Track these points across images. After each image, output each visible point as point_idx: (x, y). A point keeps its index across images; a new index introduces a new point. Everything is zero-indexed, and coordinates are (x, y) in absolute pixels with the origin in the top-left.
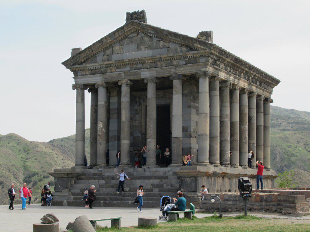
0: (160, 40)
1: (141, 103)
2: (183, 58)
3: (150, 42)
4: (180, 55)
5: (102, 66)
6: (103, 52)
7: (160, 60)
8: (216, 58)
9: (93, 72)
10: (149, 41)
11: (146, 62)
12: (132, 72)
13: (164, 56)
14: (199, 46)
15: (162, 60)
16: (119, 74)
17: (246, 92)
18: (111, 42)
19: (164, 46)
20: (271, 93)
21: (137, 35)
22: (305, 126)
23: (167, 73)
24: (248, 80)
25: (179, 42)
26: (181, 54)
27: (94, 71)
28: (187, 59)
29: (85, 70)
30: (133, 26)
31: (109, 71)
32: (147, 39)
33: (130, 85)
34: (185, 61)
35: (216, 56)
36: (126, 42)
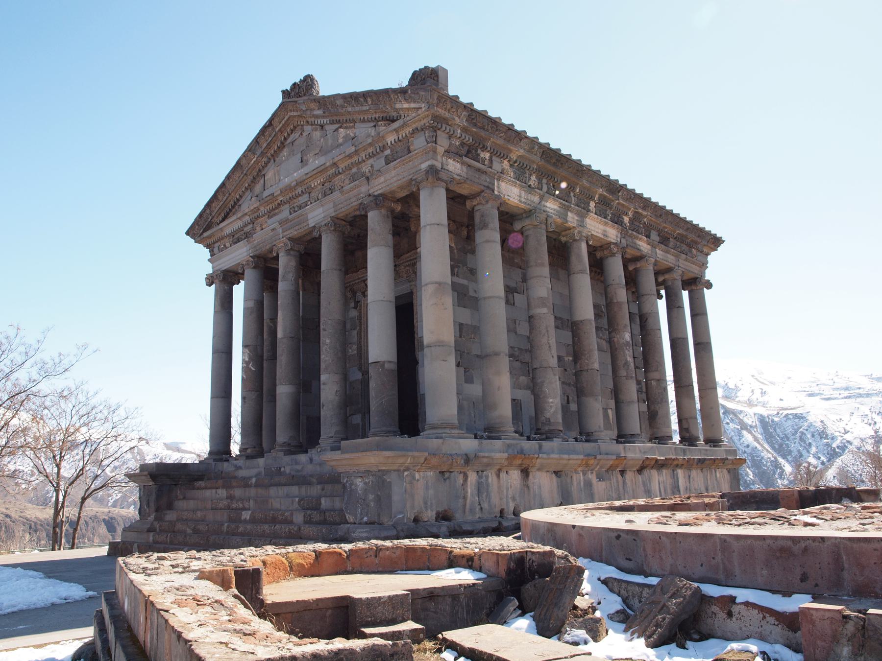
4: (370, 144)
8: (469, 139)
9: (236, 238)
10: (321, 137)
13: (340, 157)
14: (406, 105)
17: (615, 250)
18: (257, 162)
19: (346, 138)
20: (704, 265)
22: (858, 391)
24: (617, 220)
26: (370, 140)
27: (236, 236)
28: (388, 152)
29: (222, 238)
31: (258, 229)
32: (317, 134)
33: (298, 251)
35: (465, 130)
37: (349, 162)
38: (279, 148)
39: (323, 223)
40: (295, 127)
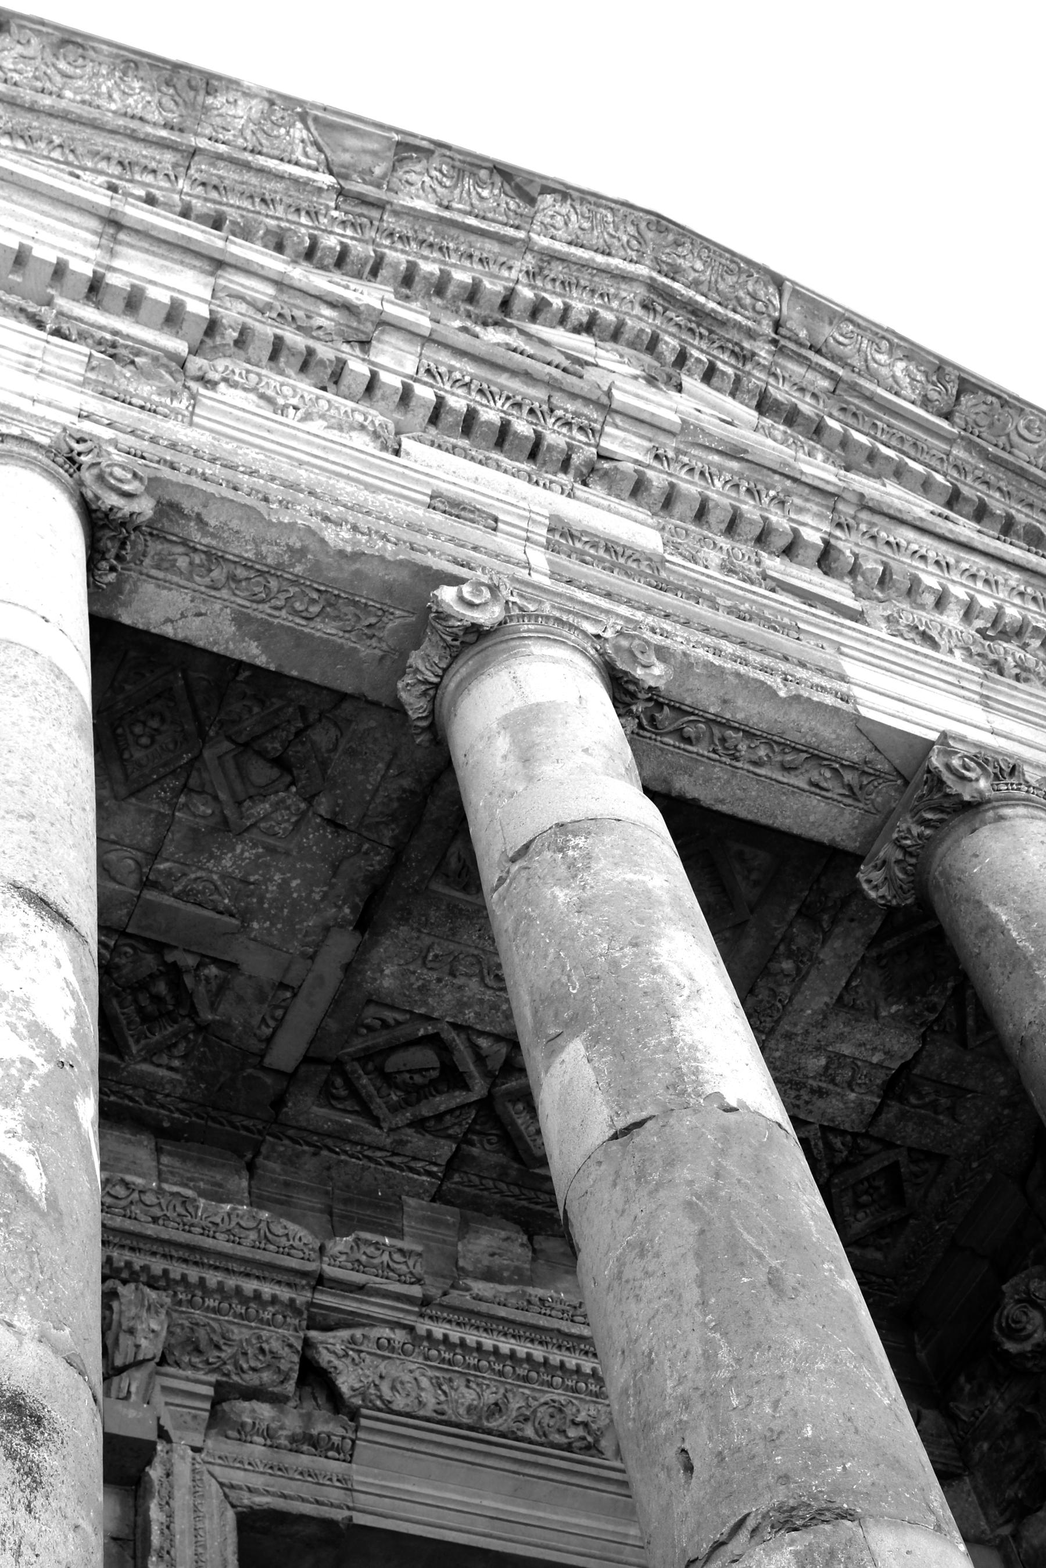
5: (132, 267)
16: (456, 508)
38: (473, 294)
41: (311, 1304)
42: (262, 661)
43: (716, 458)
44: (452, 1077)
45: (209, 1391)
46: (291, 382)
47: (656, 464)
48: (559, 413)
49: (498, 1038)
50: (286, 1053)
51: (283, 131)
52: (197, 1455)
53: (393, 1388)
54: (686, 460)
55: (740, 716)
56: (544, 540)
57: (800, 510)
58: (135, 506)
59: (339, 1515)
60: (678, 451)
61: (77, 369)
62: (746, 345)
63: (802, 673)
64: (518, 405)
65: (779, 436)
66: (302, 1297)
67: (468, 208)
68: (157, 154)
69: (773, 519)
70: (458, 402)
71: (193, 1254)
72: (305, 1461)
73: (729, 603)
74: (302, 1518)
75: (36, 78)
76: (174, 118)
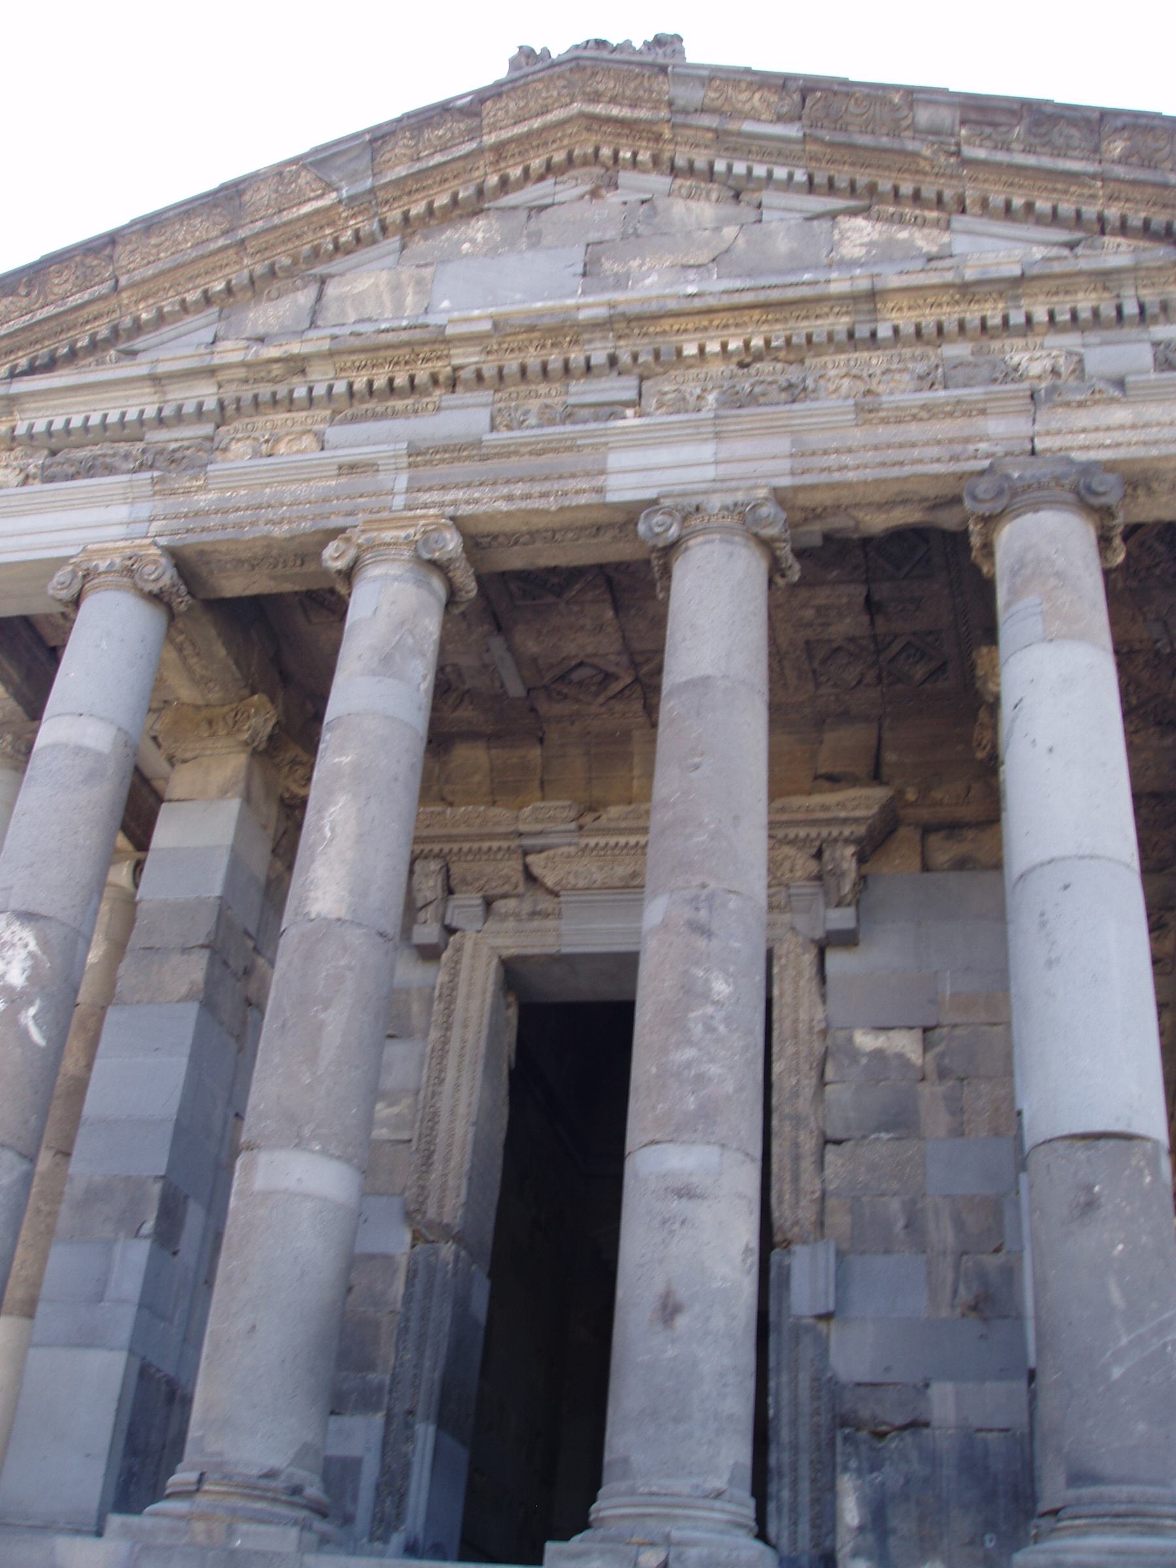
0: (852, 203)
1: (450, 931)
2: (1131, 309)
3: (729, 232)
6: (215, 310)
7: (942, 223)
11: (690, 350)
12: (505, 452)
15: (884, 331)
16: (352, 468)
21: (594, 194)
23: (935, 451)
25: (1066, 208)
30: (576, 107)
34: (1156, 344)
36: (473, 241)
37: (950, 316)
39: (715, 502)
40: (570, 161)
41: (521, 846)
42: (297, 588)
43: (524, 336)
44: (608, 677)
45: (479, 901)
46: (270, 417)
47: (490, 358)
48: (421, 356)
49: (619, 654)
50: (516, 689)
51: (293, 186)
52: (480, 935)
53: (576, 877)
54: (505, 346)
55: (541, 526)
56: (405, 465)
57: (590, 341)
58: (161, 584)
59: (553, 950)
60: (500, 344)
61: (148, 489)
62: (655, 129)
63: (571, 484)
64: (397, 363)
65: (684, 192)
66: (514, 843)
67: (432, 150)
68: (224, 255)
69: (573, 356)
70: (360, 384)
71: (450, 838)
72: (536, 924)
73: (529, 448)
74: (533, 956)
75: (143, 259)
76: (225, 226)
